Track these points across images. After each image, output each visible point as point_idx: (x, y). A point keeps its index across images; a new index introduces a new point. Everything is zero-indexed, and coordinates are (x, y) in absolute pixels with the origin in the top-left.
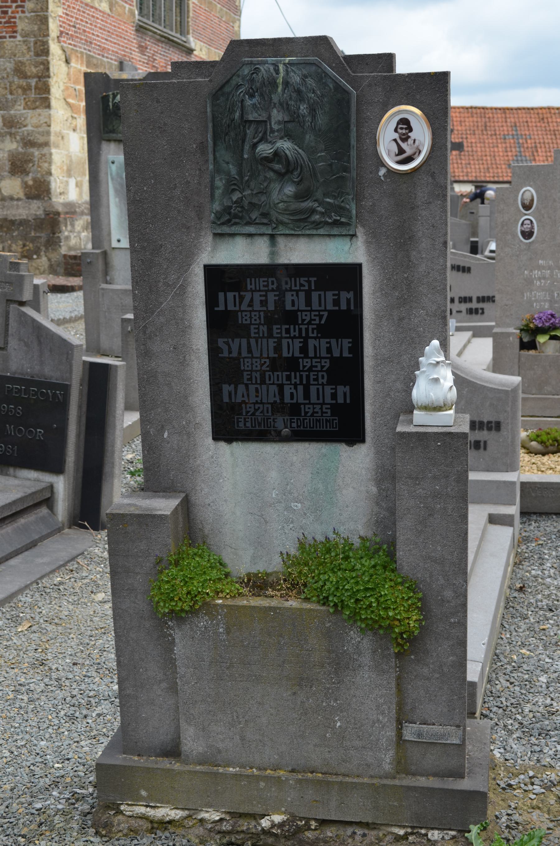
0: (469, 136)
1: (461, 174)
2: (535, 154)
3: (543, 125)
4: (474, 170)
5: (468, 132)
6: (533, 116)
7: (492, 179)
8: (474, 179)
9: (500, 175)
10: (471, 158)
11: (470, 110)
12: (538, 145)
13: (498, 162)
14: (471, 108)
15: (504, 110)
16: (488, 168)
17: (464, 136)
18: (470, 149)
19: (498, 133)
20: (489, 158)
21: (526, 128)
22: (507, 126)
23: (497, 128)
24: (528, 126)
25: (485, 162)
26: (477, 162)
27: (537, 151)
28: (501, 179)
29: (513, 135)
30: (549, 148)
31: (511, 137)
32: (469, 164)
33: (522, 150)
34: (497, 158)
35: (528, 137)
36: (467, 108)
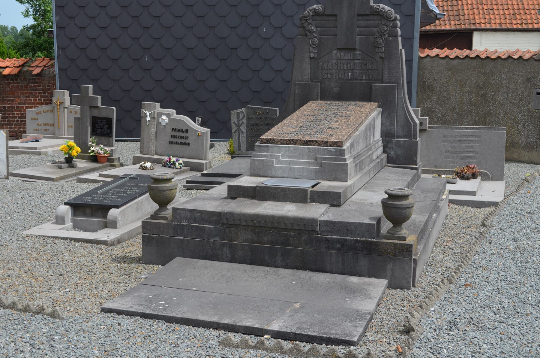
1: (483, 21)
4: (497, 17)
7: (520, 27)
8: (498, 26)
9: (530, 21)
13: (526, 7)
16: (515, 14)
25: (510, 7)
26: (500, 7)
28: (530, 27)
32: (493, 9)
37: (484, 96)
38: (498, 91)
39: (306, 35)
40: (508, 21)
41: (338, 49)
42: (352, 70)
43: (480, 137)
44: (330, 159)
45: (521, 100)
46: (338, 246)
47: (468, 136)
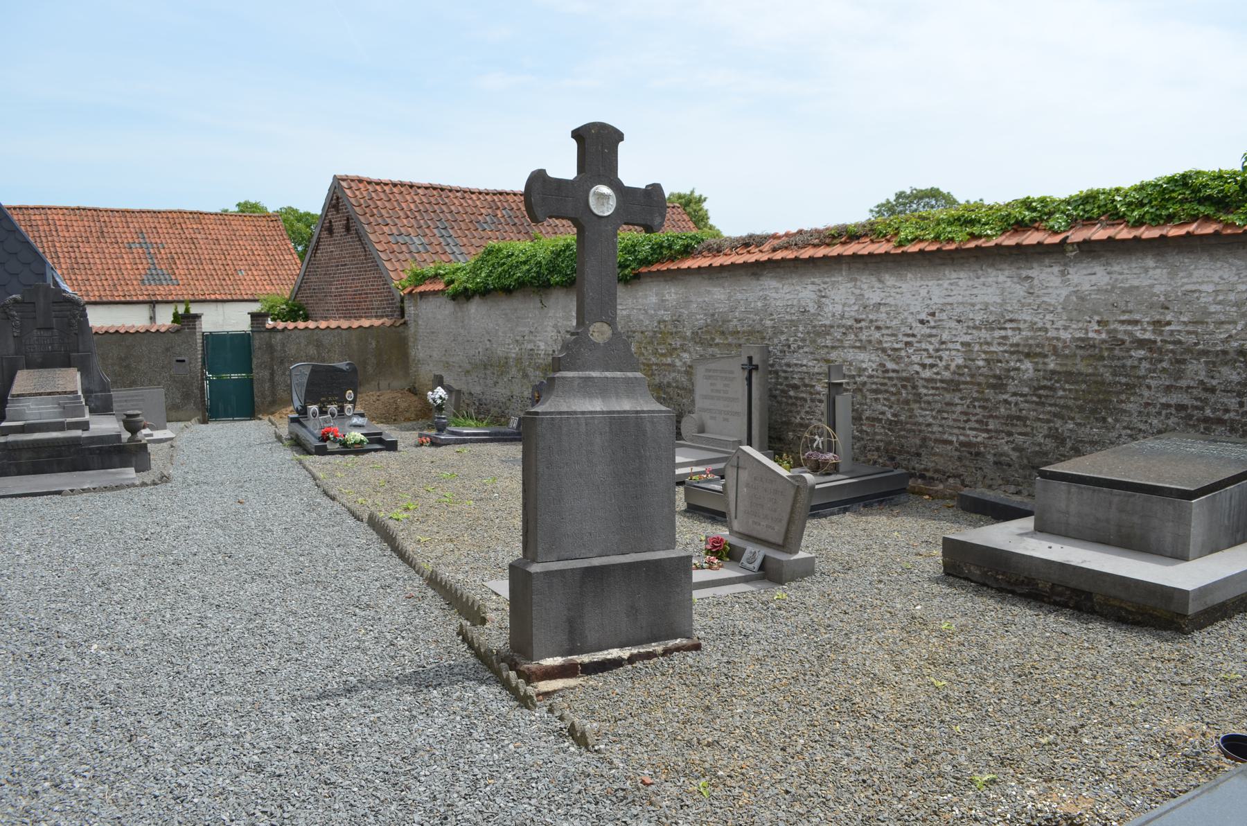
0: (81, 244)
2: (174, 266)
3: (176, 232)
4: (95, 288)
5: (79, 239)
6: (161, 220)
7: (123, 299)
8: (98, 299)
9: (133, 293)
10: (89, 272)
11: (77, 212)
12: (175, 256)
13: (127, 277)
14: (79, 209)
15: (124, 212)
16: (115, 285)
17: (75, 245)
18: (85, 261)
19: (120, 241)
20: (113, 272)
21: (156, 235)
22: (131, 232)
23: (118, 235)
24: (158, 233)
25: (108, 277)
26: (97, 278)
27: (175, 264)
28: (135, 299)
29: (140, 243)
30: (190, 259)
31: (138, 246)
32: (88, 280)
33: (156, 261)
34: (125, 273)
35: (160, 246)
36: (73, 209)
37: (127, 367)
38: (141, 361)
39: (8, 319)
40: (108, 293)
41: (38, 329)
42: (51, 344)
43: (142, 395)
44: (70, 403)
45: (163, 368)
46: (98, 452)
47: (133, 396)
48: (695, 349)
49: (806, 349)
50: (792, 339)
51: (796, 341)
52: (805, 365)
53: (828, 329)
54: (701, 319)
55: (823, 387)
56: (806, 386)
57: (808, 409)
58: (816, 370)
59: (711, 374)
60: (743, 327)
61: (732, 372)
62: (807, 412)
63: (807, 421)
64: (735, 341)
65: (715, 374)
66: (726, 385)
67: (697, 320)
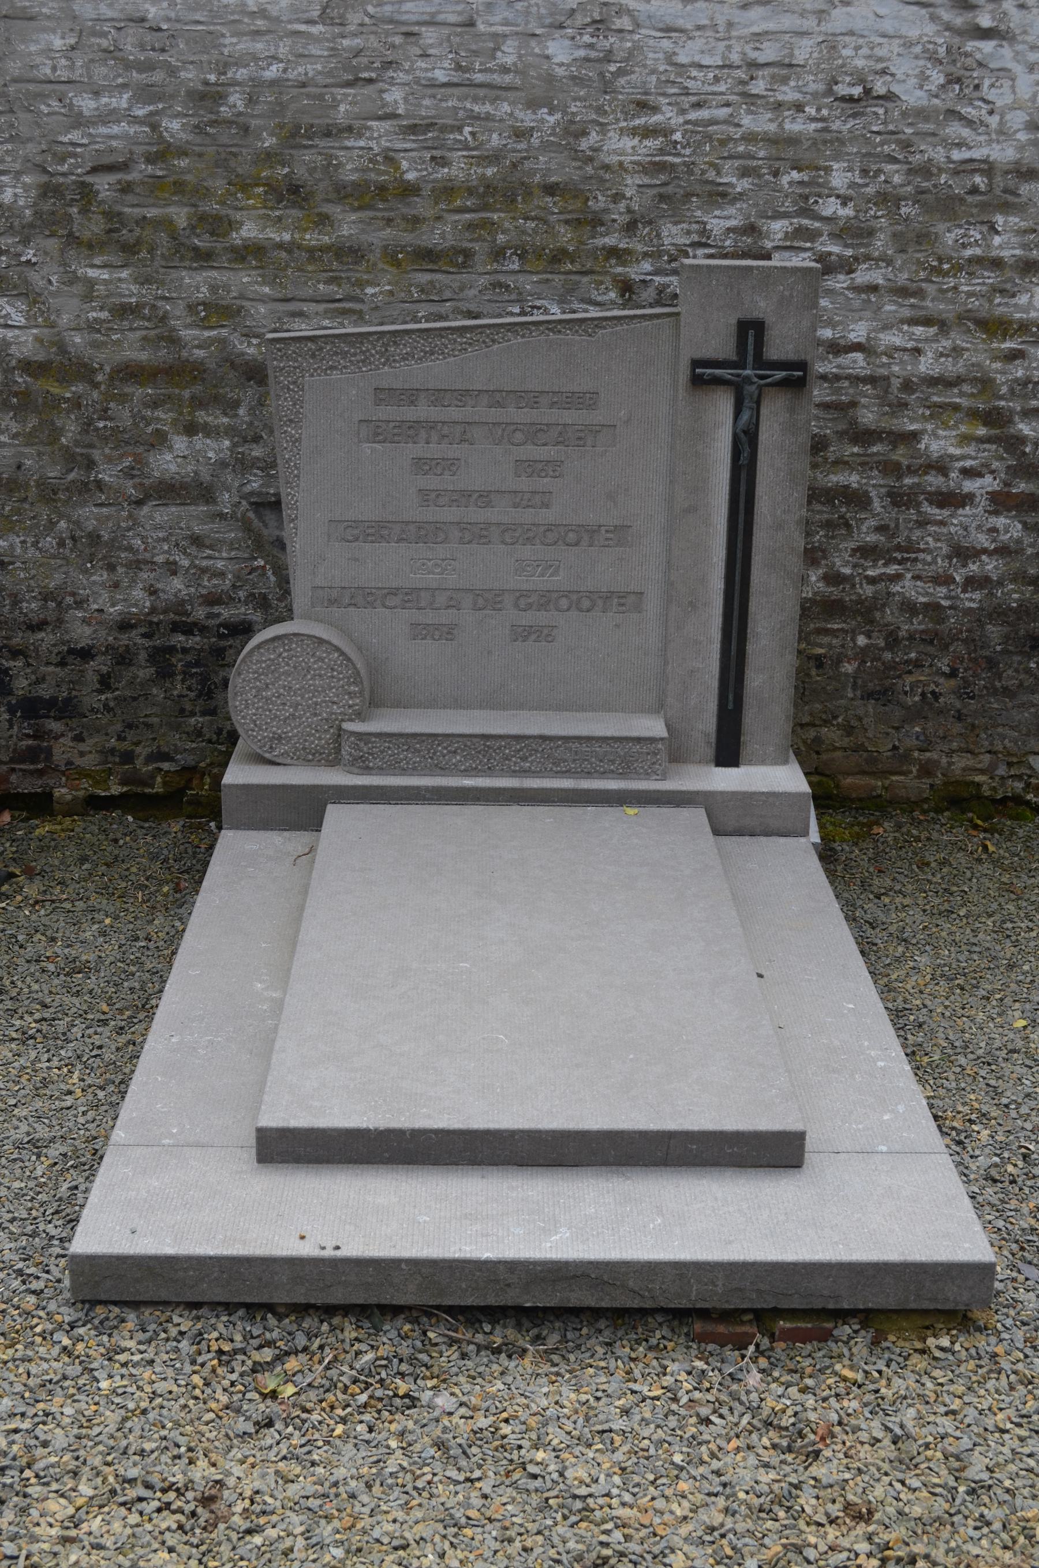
48: (72, 279)
49: (864, 275)
50: (778, 227)
51: (800, 233)
52: (858, 347)
53: (999, 181)
54: (108, 117)
55: (965, 439)
56: (864, 436)
57: (872, 538)
58: (926, 365)
59: (423, 411)
60: (441, 162)
61: (586, 400)
62: (867, 552)
63: (869, 590)
64: (381, 236)
65: (455, 413)
66: (529, 467)
67: (78, 121)
